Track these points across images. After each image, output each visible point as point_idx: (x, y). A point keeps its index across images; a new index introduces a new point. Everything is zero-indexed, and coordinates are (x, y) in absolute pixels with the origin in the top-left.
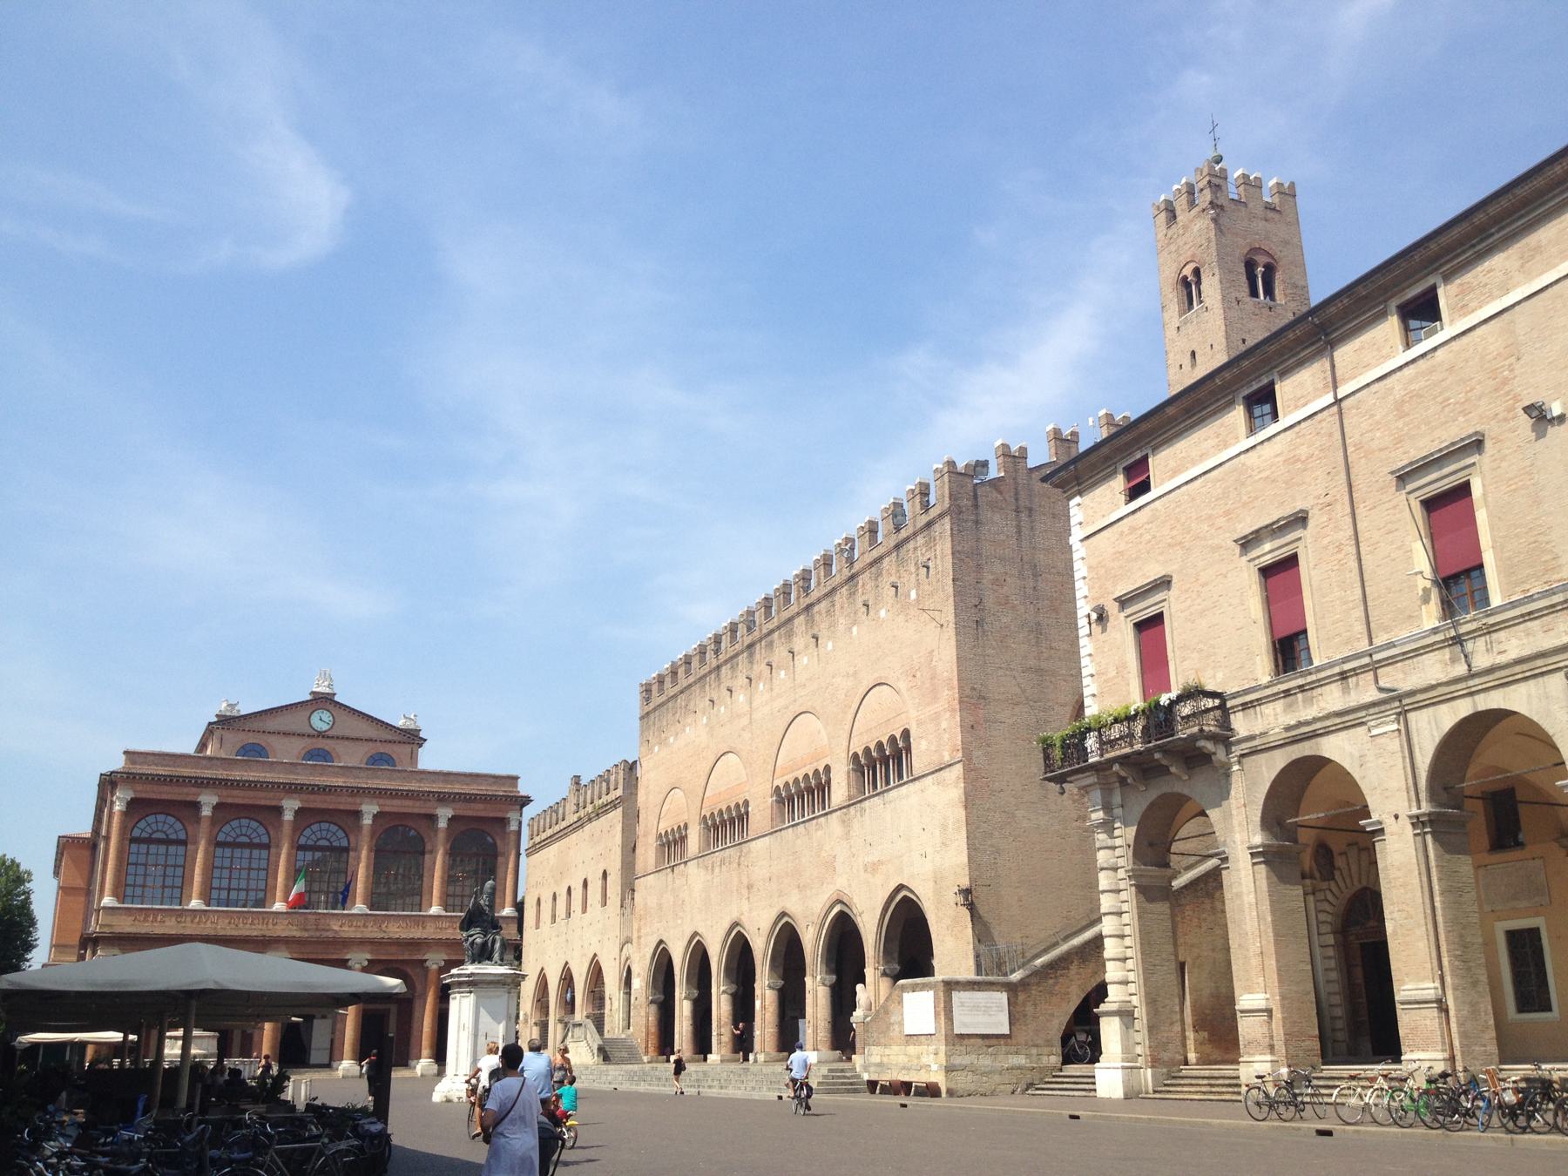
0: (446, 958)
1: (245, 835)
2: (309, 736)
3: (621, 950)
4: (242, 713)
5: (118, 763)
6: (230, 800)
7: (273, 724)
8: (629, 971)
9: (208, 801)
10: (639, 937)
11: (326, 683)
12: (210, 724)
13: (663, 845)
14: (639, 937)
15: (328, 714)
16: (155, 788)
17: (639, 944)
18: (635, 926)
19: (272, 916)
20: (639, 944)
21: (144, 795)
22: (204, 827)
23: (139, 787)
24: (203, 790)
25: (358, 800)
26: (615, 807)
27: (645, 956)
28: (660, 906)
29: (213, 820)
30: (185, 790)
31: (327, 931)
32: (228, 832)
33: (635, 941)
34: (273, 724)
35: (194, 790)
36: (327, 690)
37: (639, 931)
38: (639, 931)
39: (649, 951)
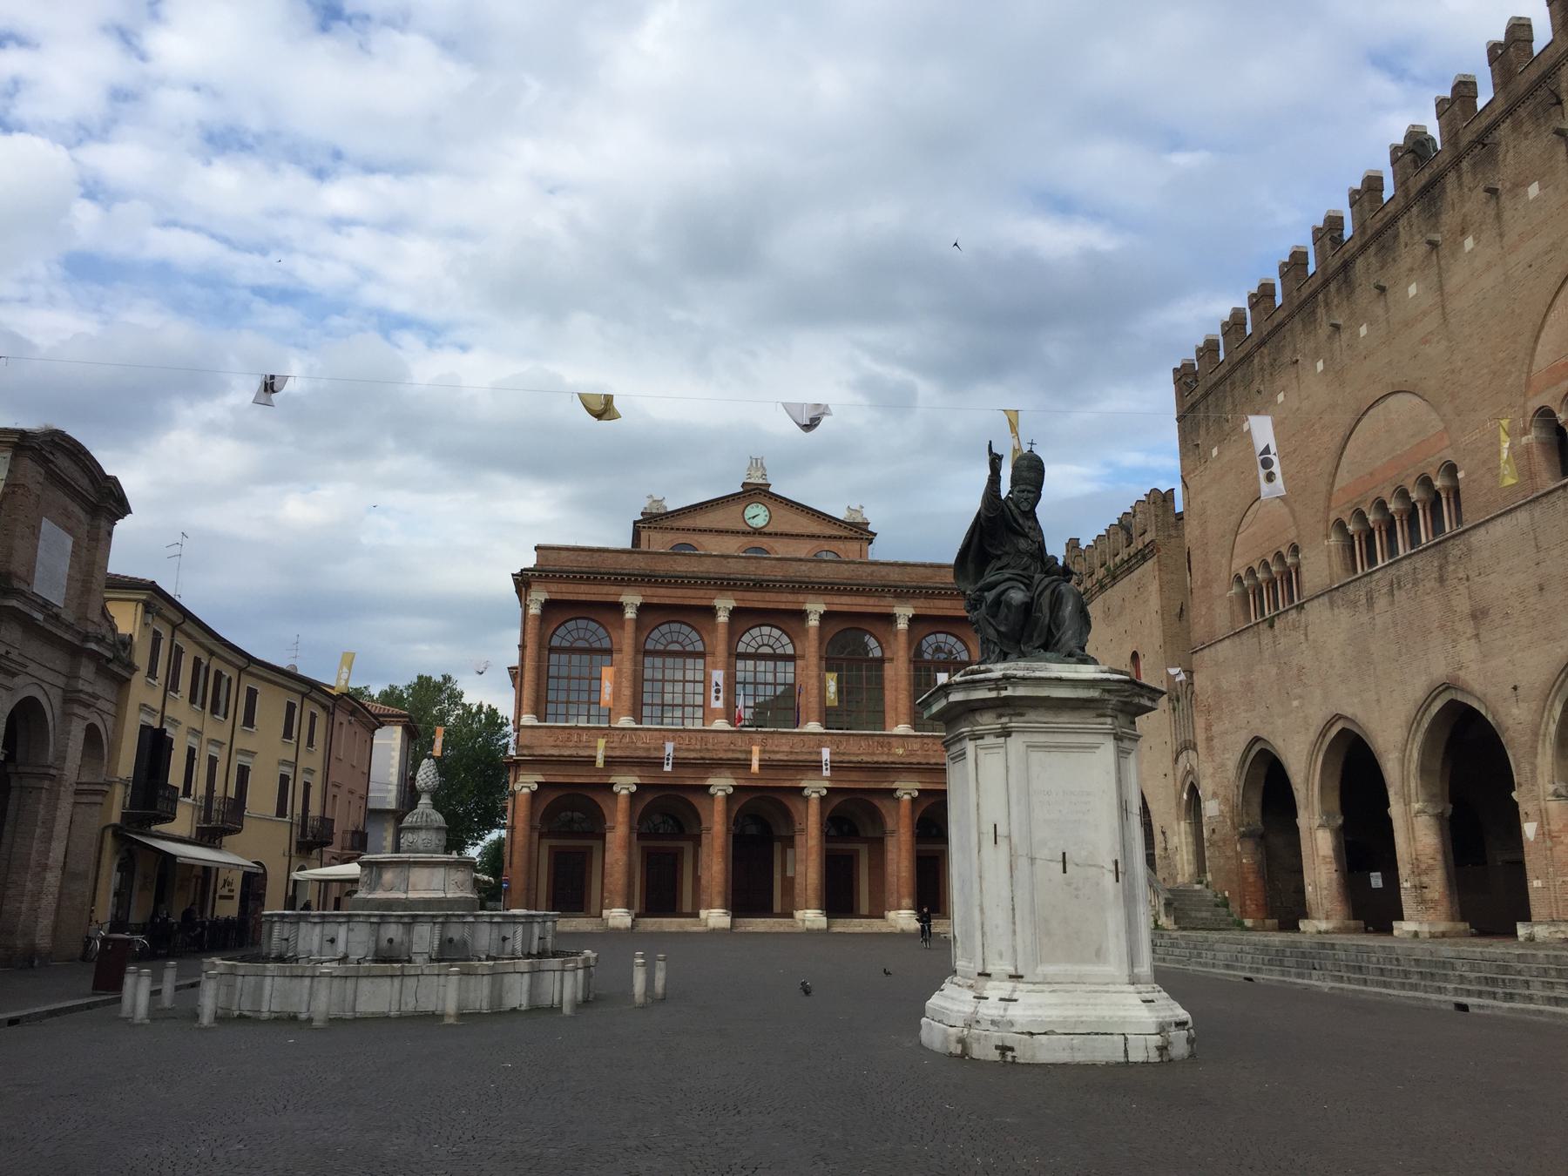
0: (920, 786)
1: (677, 642)
2: (743, 533)
3: (1176, 760)
4: (669, 509)
5: (530, 560)
6: (655, 601)
7: (702, 521)
8: (1193, 790)
9: (631, 600)
10: (1209, 739)
11: (759, 474)
12: (635, 523)
13: (1244, 595)
14: (1209, 739)
15: (764, 508)
16: (571, 588)
17: (1210, 748)
18: (1200, 722)
19: (712, 734)
20: (1210, 748)
21: (559, 597)
22: (629, 630)
23: (554, 587)
24: (626, 589)
25: (801, 598)
26: (1145, 559)
27: (1223, 765)
28: (1249, 686)
29: (638, 621)
30: (605, 589)
31: (777, 752)
32: (660, 637)
33: (1201, 746)
34: (702, 521)
35: (614, 589)
36: (761, 481)
37: (1208, 727)
38: (1208, 727)
39: (1232, 759)
